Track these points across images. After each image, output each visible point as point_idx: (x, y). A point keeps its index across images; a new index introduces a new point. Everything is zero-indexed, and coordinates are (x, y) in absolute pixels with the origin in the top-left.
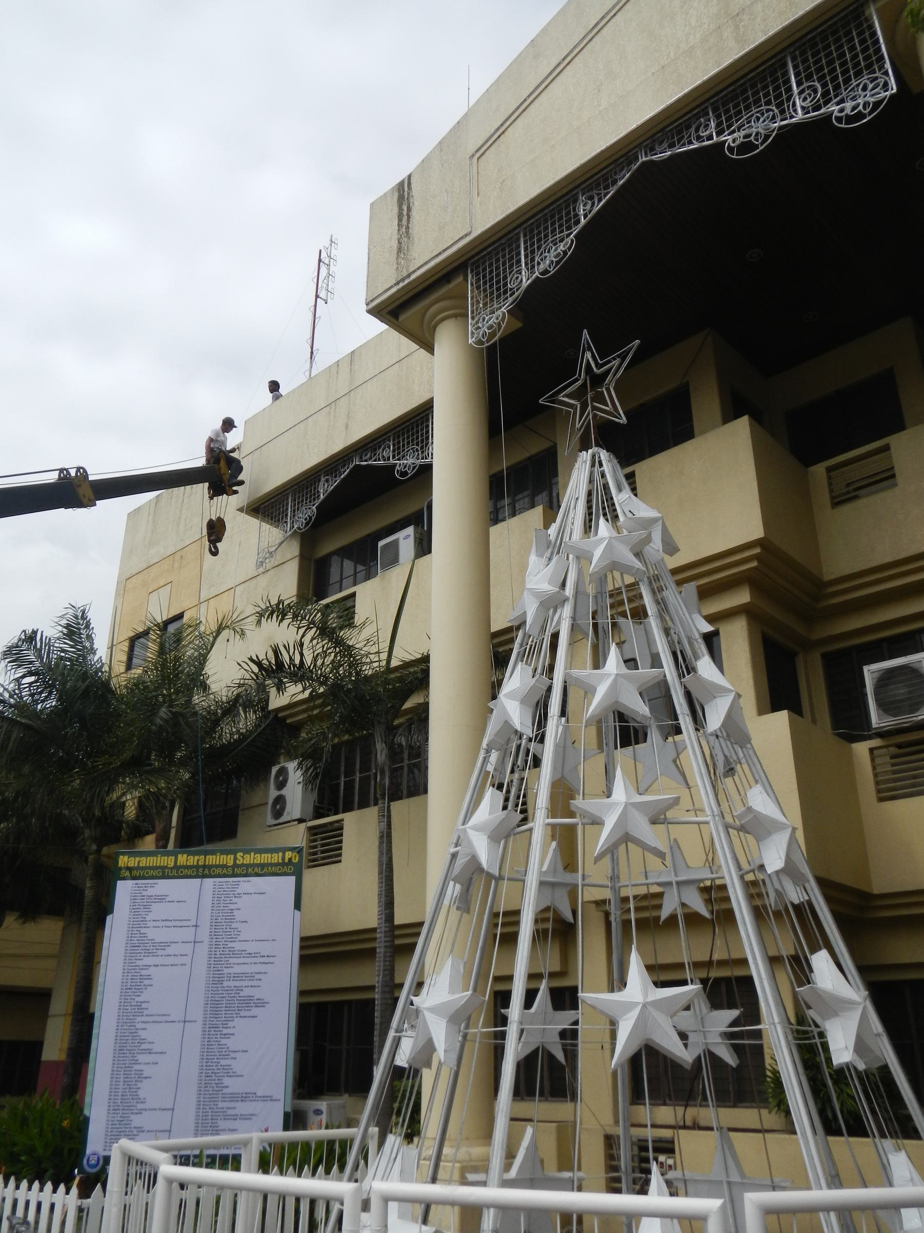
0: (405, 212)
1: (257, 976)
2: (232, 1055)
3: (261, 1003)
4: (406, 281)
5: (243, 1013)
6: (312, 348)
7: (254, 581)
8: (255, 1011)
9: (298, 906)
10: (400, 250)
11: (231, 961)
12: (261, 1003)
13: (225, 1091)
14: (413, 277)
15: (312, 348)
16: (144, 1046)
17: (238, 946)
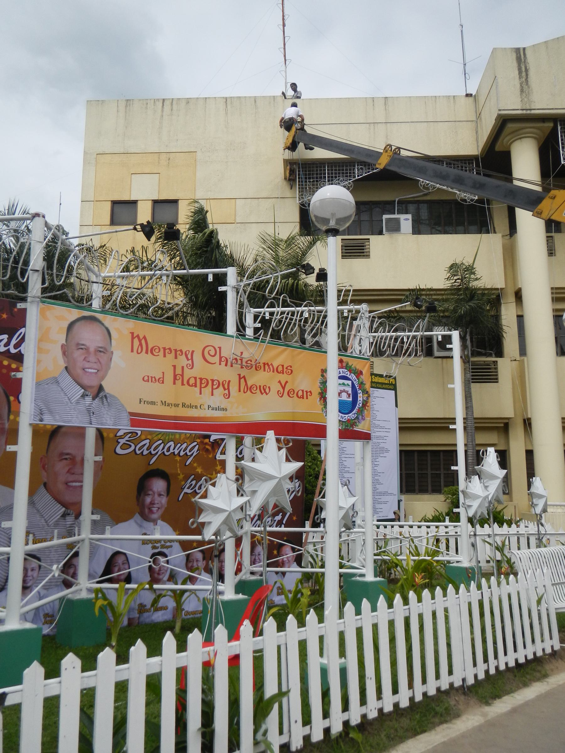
0: (523, 69)
1: (385, 438)
2: (379, 474)
3: (387, 451)
4: (528, 112)
5: (382, 455)
6: (285, 56)
7: (256, 201)
8: (386, 454)
9: (397, 406)
10: (522, 91)
11: (375, 430)
12: (387, 451)
13: (378, 491)
14: (533, 112)
15: (285, 56)
16: (346, 469)
17: (377, 423)
